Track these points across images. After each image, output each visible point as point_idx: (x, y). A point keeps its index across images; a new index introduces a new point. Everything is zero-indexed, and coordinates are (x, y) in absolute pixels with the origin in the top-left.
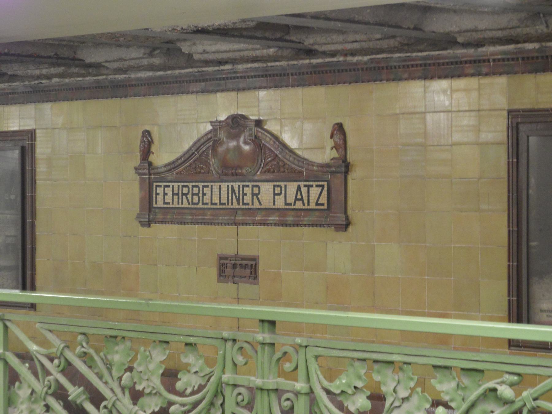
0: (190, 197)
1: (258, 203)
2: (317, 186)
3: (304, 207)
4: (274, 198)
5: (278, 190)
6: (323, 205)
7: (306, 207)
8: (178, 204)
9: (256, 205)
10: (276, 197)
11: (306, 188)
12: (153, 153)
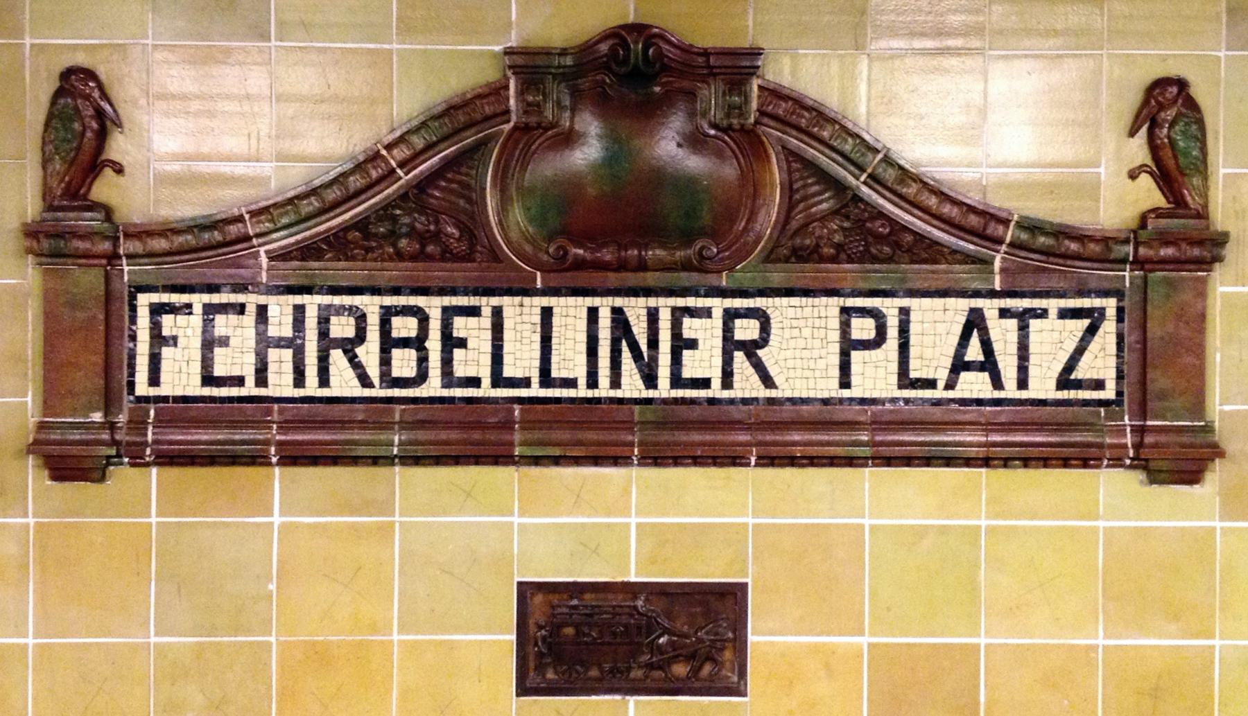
0: (369, 353)
2: (1064, 314)
3: (998, 394)
5: (863, 328)
6: (1099, 385)
7: (1011, 390)
8: (299, 380)
9: (747, 384)
10: (856, 356)
11: (1013, 324)
12: (119, 170)
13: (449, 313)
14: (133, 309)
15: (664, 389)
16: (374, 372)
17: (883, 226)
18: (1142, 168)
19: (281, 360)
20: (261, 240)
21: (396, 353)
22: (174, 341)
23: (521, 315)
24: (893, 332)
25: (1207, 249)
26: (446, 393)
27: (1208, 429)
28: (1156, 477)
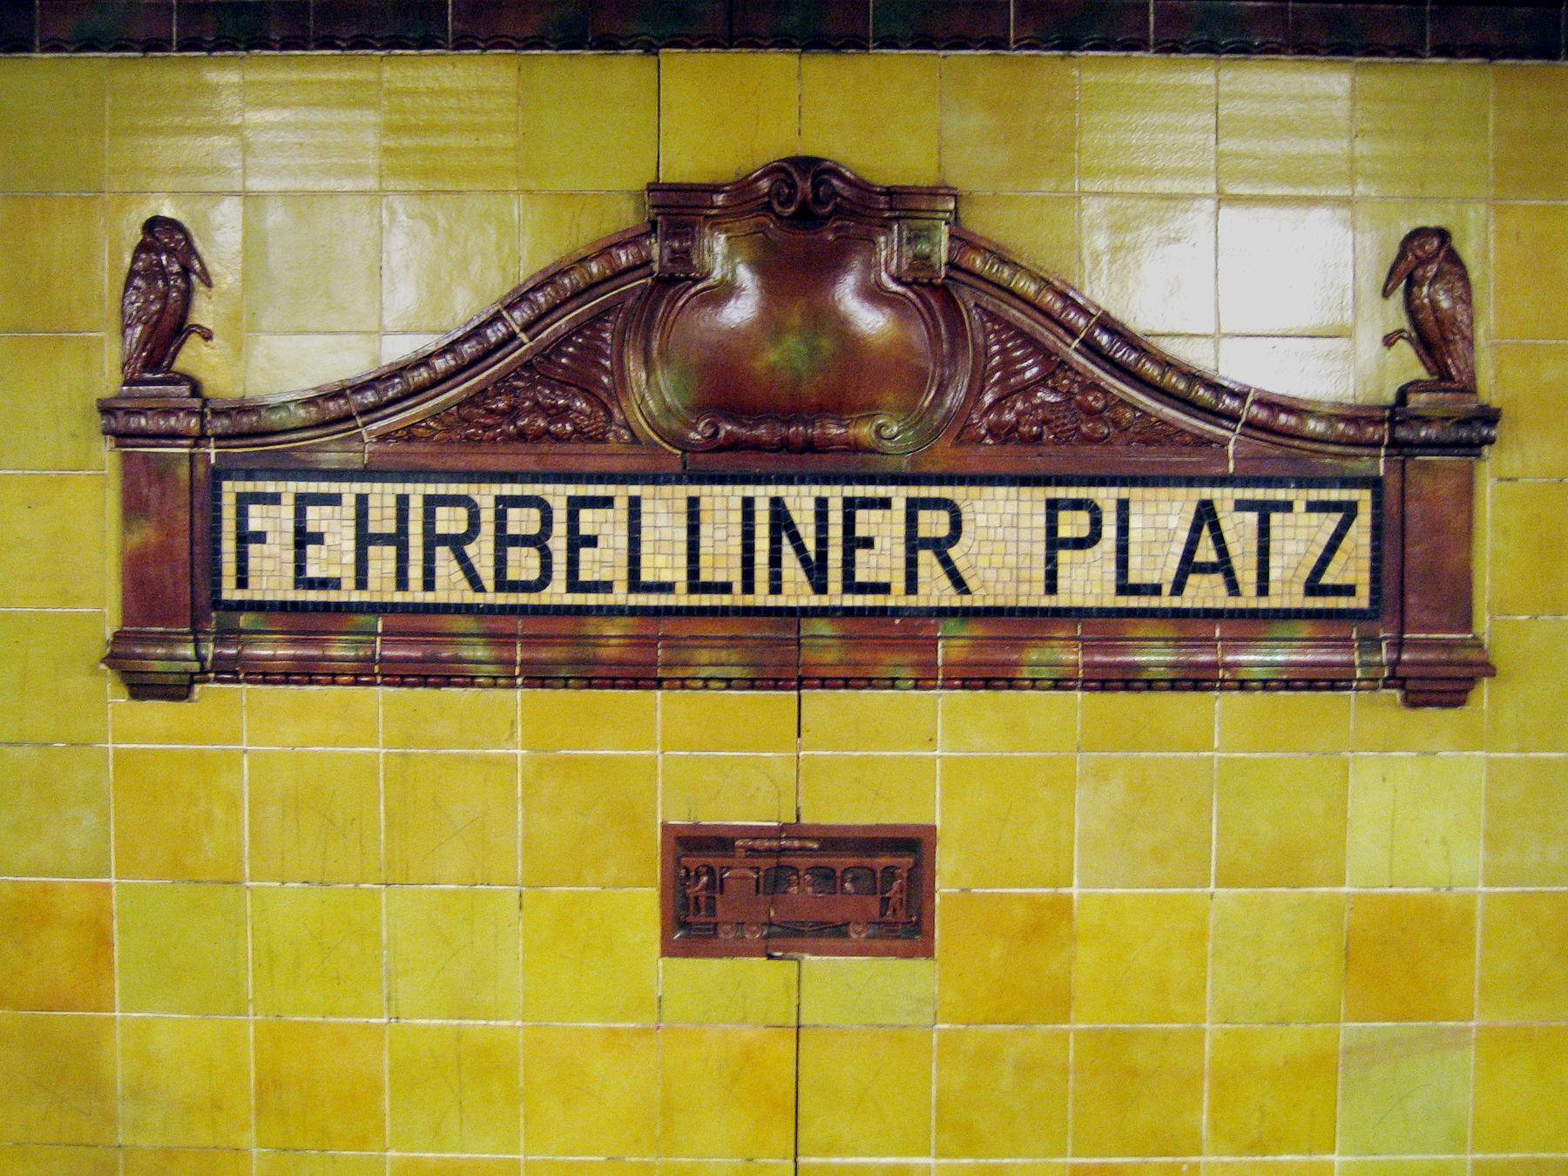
0: (482, 552)
1: (946, 582)
2: (1313, 507)
3: (1232, 603)
4: (1051, 560)
5: (1073, 524)
6: (1349, 590)
7: (1249, 599)
8: (402, 583)
9: (935, 589)
10: (1064, 556)
11: (1252, 518)
13: (575, 505)
14: (218, 497)
15: (835, 596)
16: (487, 574)
17: (1096, 399)
18: (1399, 334)
19: (382, 560)
20: (365, 419)
21: (513, 553)
22: (260, 537)
23: (663, 509)
24: (1109, 531)
25: (1475, 430)
27: (1478, 645)
28: (1414, 700)
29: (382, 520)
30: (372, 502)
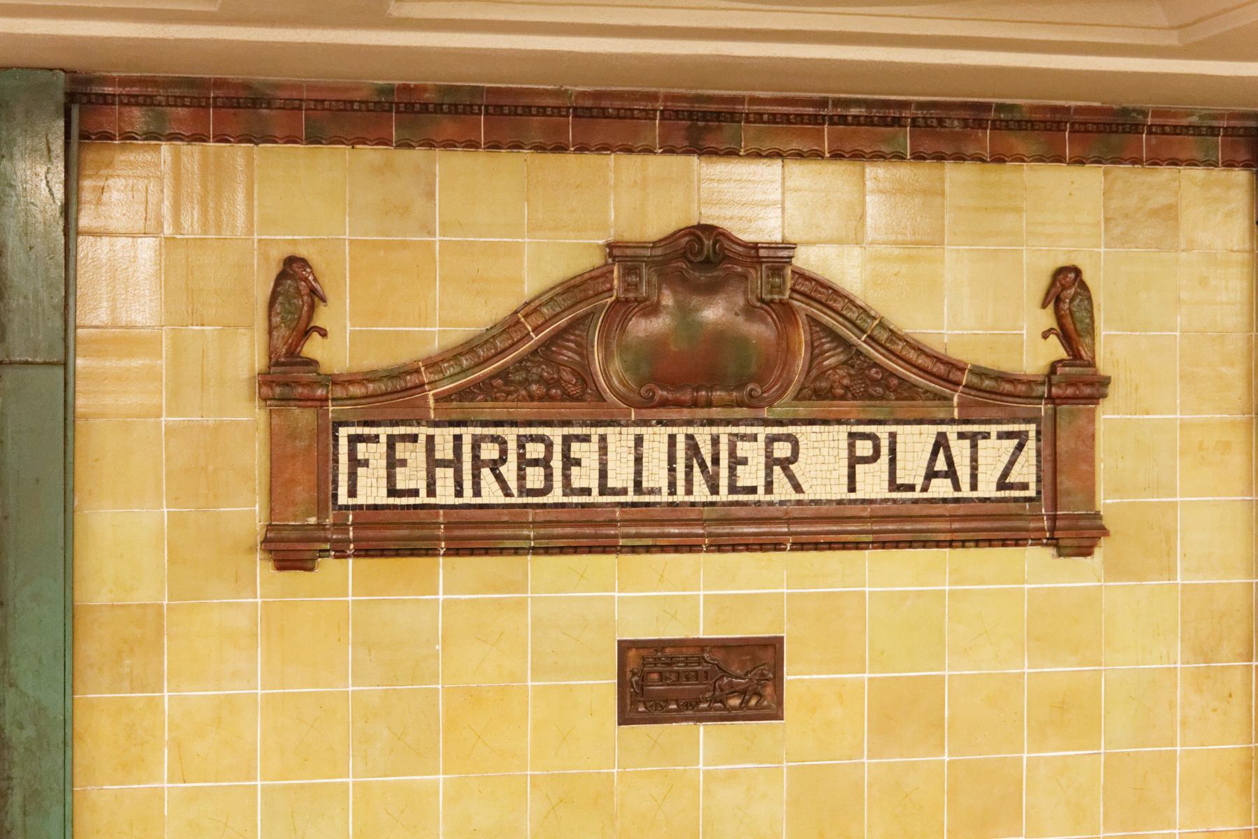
0: (509, 471)
1: (789, 486)
2: (1000, 436)
3: (957, 495)
4: (852, 468)
5: (864, 448)
6: (1025, 486)
7: (966, 492)
8: (459, 493)
9: (783, 491)
11: (967, 443)
12: (323, 333)
13: (567, 440)
14: (336, 439)
15: (724, 495)
16: (513, 485)
18: (1050, 331)
19: (445, 477)
22: (366, 463)
23: (620, 440)
24: (885, 451)
26: (565, 500)
28: (1062, 552)
29: (444, 450)
30: (437, 440)
